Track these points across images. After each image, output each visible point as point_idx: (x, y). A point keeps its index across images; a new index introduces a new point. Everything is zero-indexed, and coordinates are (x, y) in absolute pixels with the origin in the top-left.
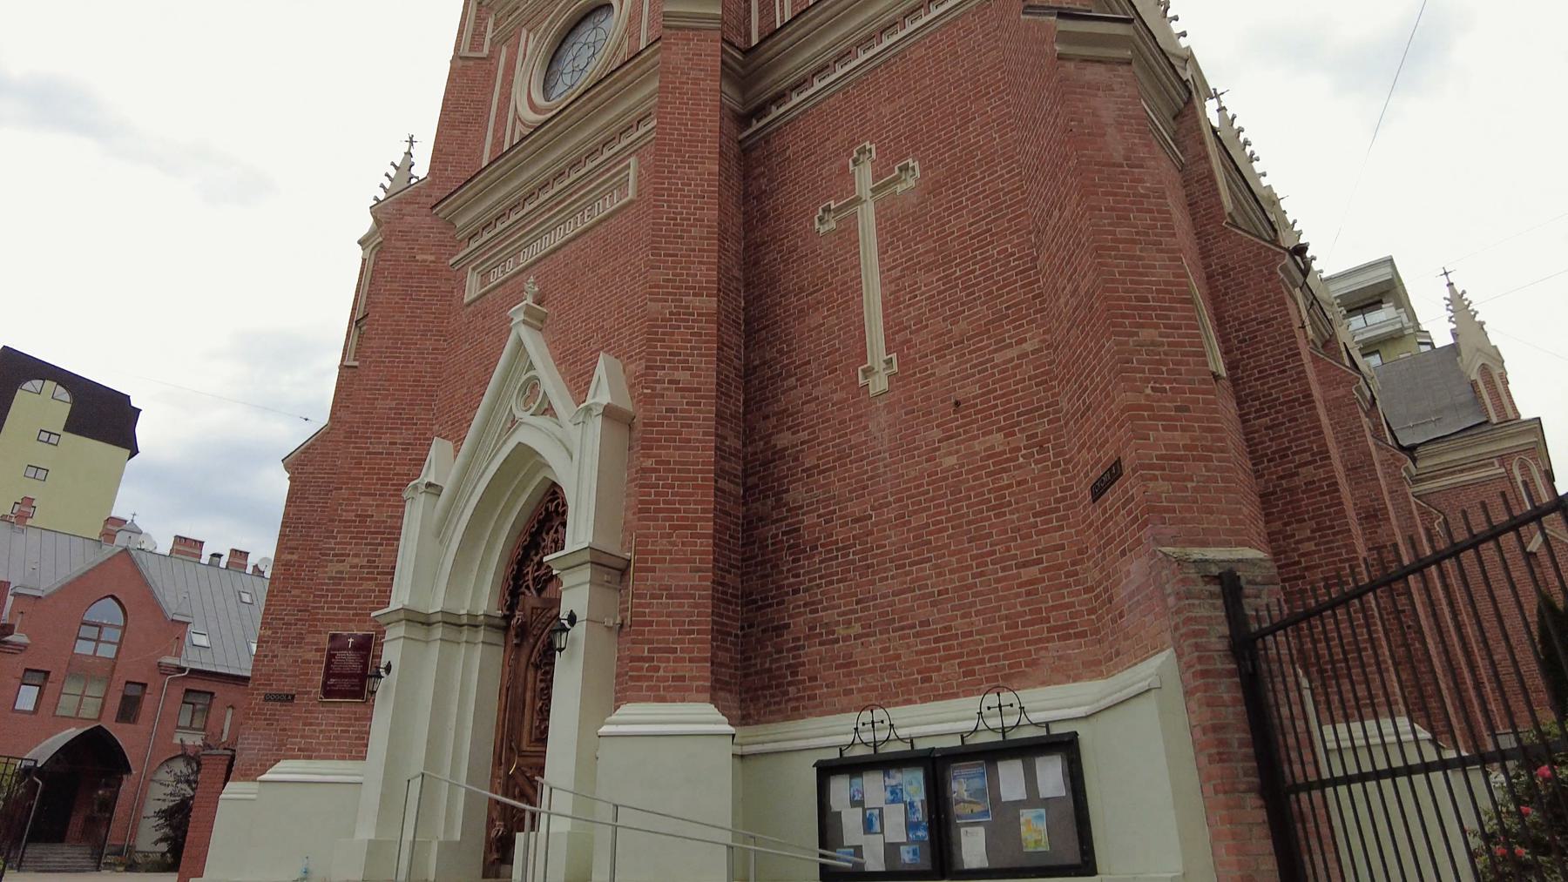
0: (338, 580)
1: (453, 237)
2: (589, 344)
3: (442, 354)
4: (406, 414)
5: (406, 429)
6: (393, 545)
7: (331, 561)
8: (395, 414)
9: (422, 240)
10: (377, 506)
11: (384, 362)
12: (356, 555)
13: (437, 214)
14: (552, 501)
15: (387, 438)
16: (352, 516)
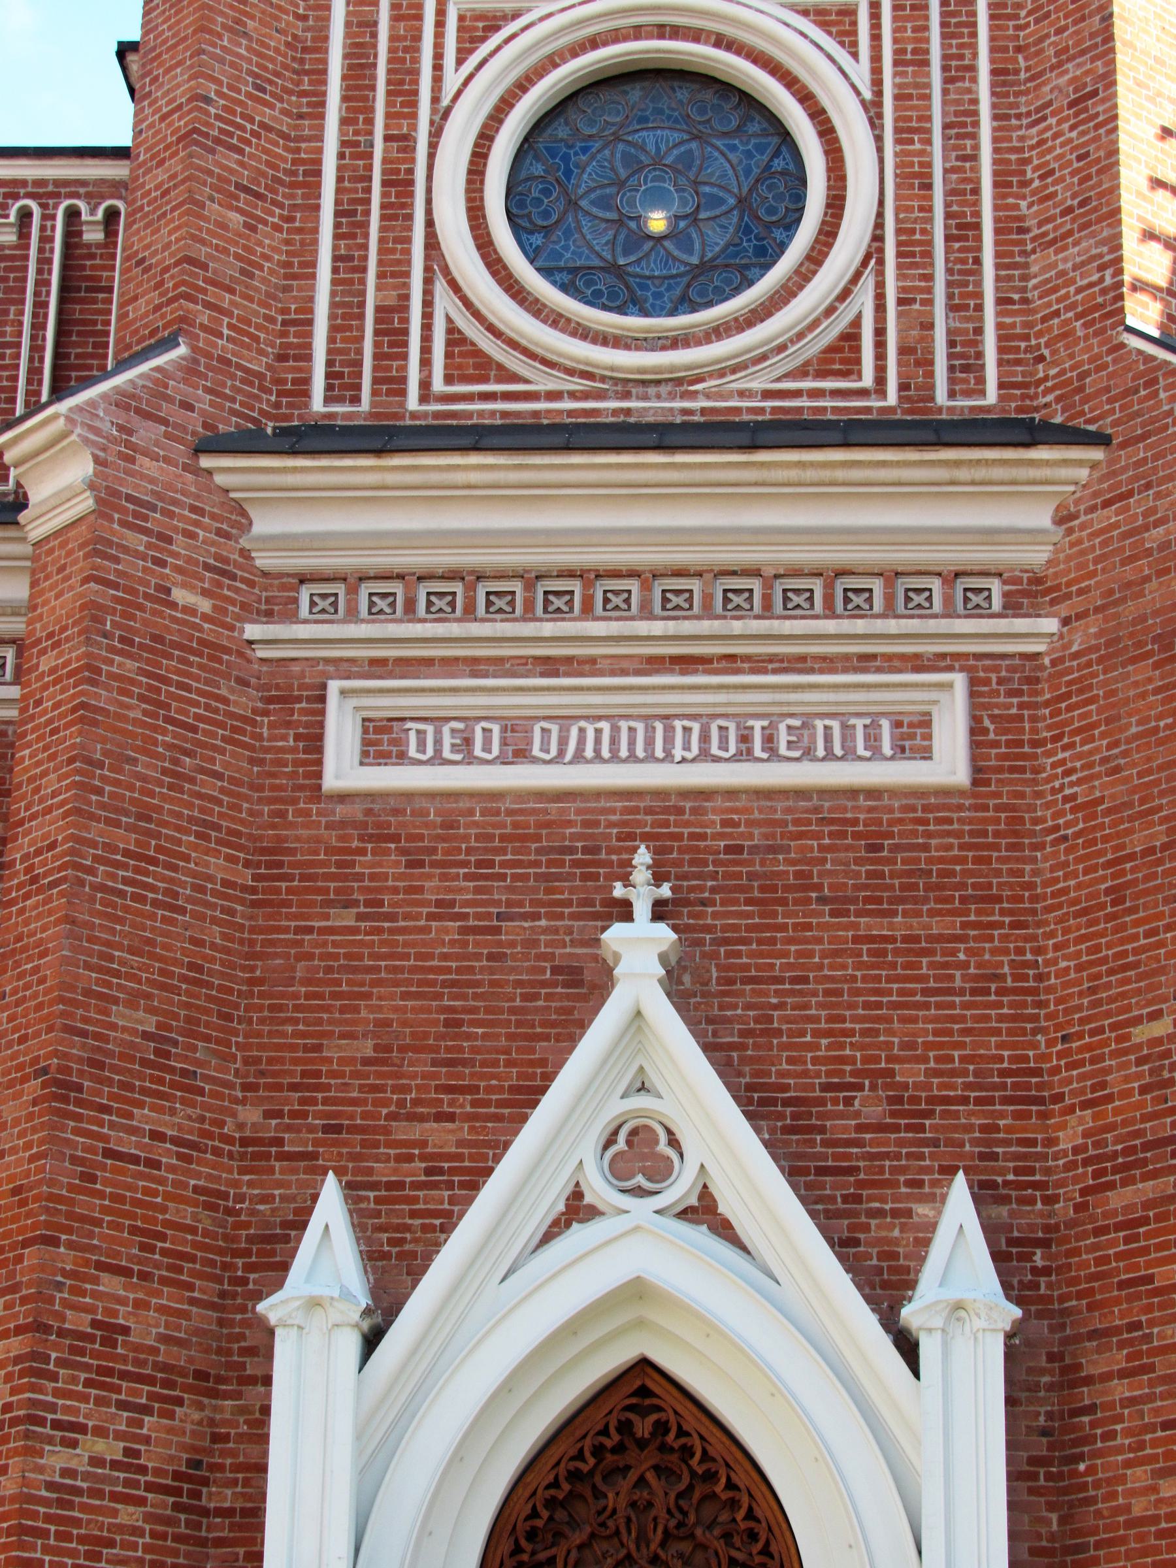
0: (64, 1494)
1: (245, 553)
2: (849, 1101)
3: (242, 902)
4: (178, 1057)
5: (183, 1101)
6: (171, 1415)
7: (50, 1440)
8: (157, 1052)
9: (180, 545)
10: (139, 1304)
11: (122, 894)
12: (100, 1432)
13: (209, 472)
14: (644, 1412)
15: (145, 1118)
16: (79, 1322)
